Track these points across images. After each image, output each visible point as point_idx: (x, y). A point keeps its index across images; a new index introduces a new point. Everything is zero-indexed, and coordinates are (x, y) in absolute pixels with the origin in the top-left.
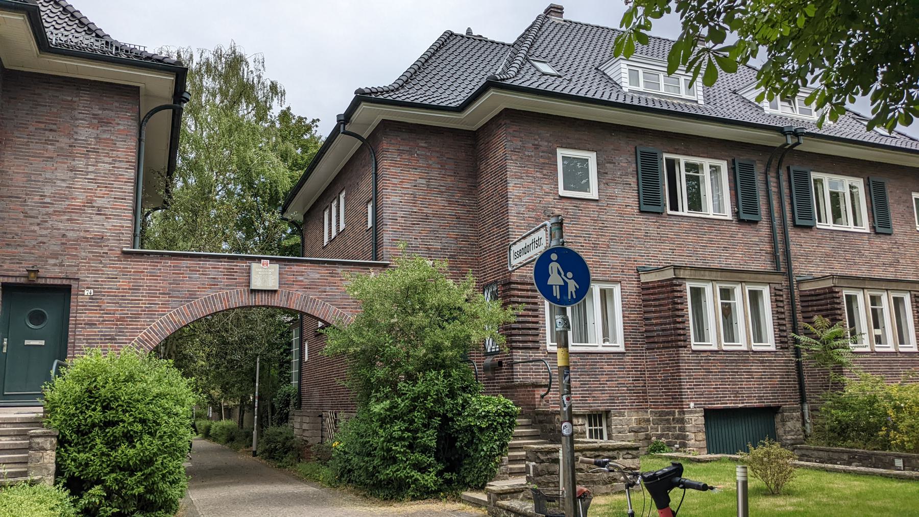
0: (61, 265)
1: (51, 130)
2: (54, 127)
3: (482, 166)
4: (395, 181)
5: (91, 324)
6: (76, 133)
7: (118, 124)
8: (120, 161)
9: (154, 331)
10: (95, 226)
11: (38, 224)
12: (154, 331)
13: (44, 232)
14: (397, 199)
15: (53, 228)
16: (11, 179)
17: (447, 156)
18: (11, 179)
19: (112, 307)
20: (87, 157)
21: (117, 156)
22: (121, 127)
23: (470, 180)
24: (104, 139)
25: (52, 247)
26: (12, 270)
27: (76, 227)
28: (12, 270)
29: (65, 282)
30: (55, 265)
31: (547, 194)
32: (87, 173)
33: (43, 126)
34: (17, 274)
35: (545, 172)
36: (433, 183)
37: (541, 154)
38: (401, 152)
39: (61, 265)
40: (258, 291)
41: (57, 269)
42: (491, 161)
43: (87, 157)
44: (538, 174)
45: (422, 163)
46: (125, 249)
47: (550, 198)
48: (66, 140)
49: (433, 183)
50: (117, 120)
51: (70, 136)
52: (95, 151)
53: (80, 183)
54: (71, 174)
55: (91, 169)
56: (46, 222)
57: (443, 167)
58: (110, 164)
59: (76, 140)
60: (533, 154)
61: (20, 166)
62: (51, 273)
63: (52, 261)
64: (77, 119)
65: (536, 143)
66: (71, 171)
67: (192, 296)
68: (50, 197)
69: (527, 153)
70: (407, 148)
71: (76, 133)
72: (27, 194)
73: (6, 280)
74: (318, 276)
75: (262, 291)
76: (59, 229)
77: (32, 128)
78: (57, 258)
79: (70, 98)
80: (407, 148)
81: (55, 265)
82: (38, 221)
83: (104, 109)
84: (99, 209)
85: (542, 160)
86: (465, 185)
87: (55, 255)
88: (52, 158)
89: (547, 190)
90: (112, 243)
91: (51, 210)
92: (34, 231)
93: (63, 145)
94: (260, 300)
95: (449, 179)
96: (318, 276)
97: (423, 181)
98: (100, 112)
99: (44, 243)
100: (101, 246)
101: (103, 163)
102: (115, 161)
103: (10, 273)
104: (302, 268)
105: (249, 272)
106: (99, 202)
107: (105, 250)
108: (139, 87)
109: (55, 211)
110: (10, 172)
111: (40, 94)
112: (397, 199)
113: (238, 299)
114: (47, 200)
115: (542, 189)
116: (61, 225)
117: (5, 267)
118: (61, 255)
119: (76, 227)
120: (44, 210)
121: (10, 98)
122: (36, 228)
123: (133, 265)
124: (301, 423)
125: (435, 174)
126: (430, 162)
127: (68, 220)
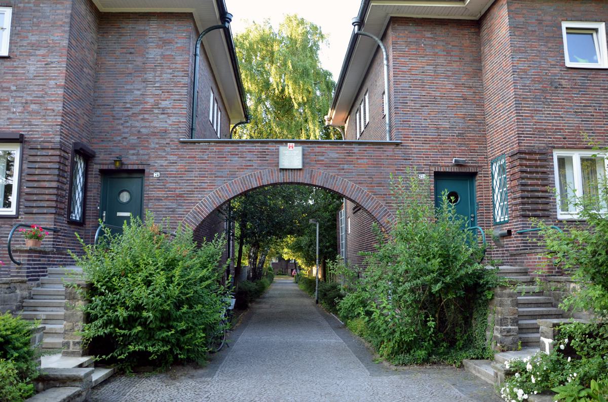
0: (138, 154)
1: (131, 53)
2: (132, 51)
3: (486, 50)
4: (405, 69)
5: (159, 199)
6: (148, 53)
7: (177, 43)
8: (178, 71)
9: (204, 204)
10: (159, 123)
11: (122, 124)
12: (204, 204)
13: (126, 130)
14: (407, 85)
15: (132, 126)
16: (104, 92)
17: (452, 44)
18: (104, 92)
19: (173, 186)
20: (155, 70)
21: (176, 68)
22: (179, 45)
23: (476, 64)
24: (167, 55)
25: (132, 141)
26: (106, 160)
27: (147, 124)
28: (106, 160)
29: (141, 167)
30: (134, 154)
31: (554, 66)
32: (155, 83)
33: (125, 50)
34: (109, 162)
35: (550, 45)
36: (440, 69)
37: (544, 28)
38: (408, 44)
39: (138, 154)
40: (286, 169)
41: (135, 157)
42: (494, 42)
43: (155, 70)
44: (543, 48)
45: (429, 51)
46: (181, 140)
47: (556, 70)
48: (140, 59)
49: (440, 69)
50: (176, 40)
51: (143, 56)
52: (161, 65)
53: (151, 90)
54: (144, 85)
55: (158, 79)
56: (127, 122)
57: (448, 53)
58: (171, 74)
59: (147, 58)
60: (536, 29)
61: (111, 82)
62: (131, 161)
63: (131, 152)
64: (148, 43)
65: (540, 18)
66: (144, 82)
67: (233, 175)
68: (130, 103)
69: (530, 28)
70: (414, 40)
71: (148, 53)
72: (115, 103)
73: (102, 167)
74: (337, 155)
75: (289, 169)
76: (136, 127)
77: (118, 53)
78: (135, 149)
79: (143, 28)
80: (414, 40)
81: (134, 154)
82: (122, 122)
83: (167, 33)
84: (163, 109)
85: (546, 34)
86: (470, 70)
87: (133, 147)
88: (131, 74)
89: (553, 63)
90: (173, 136)
91: (130, 113)
92: (120, 130)
93: (138, 63)
94: (289, 177)
95: (455, 65)
96: (337, 155)
97: (431, 68)
98: (164, 35)
99: (126, 138)
100: (165, 139)
101: (166, 73)
102: (174, 71)
103: (104, 162)
104: (322, 150)
105: (277, 154)
106: (163, 104)
107: (168, 141)
108: (192, 13)
109: (133, 114)
110: (104, 87)
111: (124, 28)
112: (407, 85)
113: (269, 177)
114: (128, 105)
115: (547, 62)
116: (137, 124)
117: (101, 158)
118: (138, 146)
119: (147, 124)
120: (126, 113)
121: (104, 33)
122: (121, 127)
123: (186, 151)
124: (76, 217)
125: (441, 60)
126: (437, 50)
127: (142, 119)
